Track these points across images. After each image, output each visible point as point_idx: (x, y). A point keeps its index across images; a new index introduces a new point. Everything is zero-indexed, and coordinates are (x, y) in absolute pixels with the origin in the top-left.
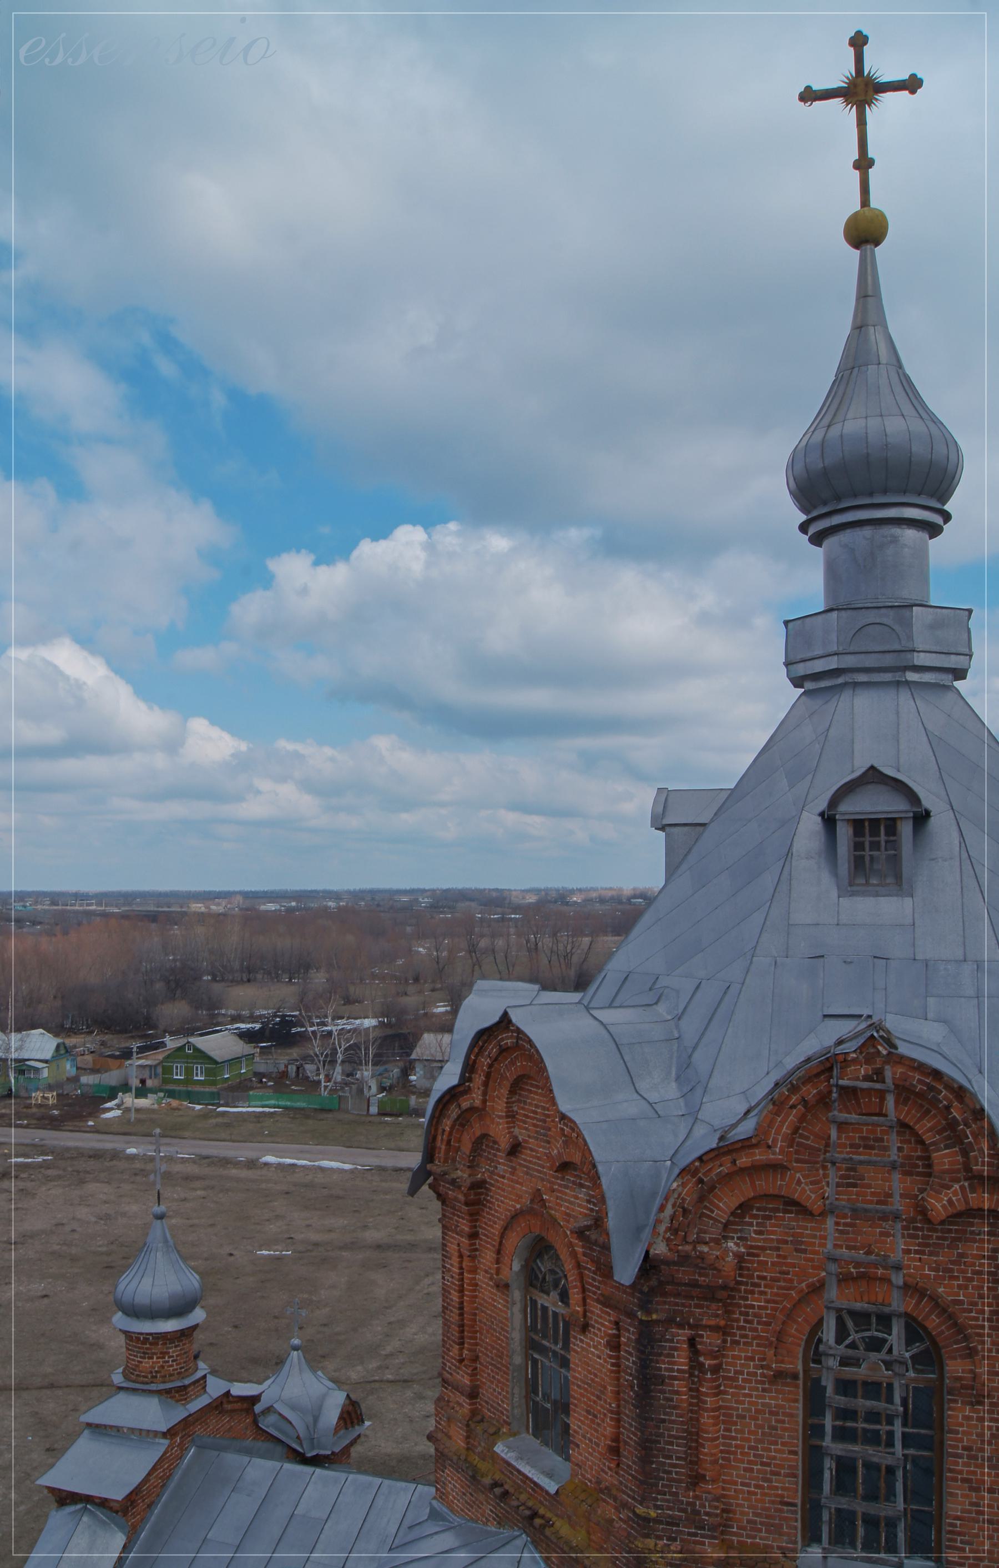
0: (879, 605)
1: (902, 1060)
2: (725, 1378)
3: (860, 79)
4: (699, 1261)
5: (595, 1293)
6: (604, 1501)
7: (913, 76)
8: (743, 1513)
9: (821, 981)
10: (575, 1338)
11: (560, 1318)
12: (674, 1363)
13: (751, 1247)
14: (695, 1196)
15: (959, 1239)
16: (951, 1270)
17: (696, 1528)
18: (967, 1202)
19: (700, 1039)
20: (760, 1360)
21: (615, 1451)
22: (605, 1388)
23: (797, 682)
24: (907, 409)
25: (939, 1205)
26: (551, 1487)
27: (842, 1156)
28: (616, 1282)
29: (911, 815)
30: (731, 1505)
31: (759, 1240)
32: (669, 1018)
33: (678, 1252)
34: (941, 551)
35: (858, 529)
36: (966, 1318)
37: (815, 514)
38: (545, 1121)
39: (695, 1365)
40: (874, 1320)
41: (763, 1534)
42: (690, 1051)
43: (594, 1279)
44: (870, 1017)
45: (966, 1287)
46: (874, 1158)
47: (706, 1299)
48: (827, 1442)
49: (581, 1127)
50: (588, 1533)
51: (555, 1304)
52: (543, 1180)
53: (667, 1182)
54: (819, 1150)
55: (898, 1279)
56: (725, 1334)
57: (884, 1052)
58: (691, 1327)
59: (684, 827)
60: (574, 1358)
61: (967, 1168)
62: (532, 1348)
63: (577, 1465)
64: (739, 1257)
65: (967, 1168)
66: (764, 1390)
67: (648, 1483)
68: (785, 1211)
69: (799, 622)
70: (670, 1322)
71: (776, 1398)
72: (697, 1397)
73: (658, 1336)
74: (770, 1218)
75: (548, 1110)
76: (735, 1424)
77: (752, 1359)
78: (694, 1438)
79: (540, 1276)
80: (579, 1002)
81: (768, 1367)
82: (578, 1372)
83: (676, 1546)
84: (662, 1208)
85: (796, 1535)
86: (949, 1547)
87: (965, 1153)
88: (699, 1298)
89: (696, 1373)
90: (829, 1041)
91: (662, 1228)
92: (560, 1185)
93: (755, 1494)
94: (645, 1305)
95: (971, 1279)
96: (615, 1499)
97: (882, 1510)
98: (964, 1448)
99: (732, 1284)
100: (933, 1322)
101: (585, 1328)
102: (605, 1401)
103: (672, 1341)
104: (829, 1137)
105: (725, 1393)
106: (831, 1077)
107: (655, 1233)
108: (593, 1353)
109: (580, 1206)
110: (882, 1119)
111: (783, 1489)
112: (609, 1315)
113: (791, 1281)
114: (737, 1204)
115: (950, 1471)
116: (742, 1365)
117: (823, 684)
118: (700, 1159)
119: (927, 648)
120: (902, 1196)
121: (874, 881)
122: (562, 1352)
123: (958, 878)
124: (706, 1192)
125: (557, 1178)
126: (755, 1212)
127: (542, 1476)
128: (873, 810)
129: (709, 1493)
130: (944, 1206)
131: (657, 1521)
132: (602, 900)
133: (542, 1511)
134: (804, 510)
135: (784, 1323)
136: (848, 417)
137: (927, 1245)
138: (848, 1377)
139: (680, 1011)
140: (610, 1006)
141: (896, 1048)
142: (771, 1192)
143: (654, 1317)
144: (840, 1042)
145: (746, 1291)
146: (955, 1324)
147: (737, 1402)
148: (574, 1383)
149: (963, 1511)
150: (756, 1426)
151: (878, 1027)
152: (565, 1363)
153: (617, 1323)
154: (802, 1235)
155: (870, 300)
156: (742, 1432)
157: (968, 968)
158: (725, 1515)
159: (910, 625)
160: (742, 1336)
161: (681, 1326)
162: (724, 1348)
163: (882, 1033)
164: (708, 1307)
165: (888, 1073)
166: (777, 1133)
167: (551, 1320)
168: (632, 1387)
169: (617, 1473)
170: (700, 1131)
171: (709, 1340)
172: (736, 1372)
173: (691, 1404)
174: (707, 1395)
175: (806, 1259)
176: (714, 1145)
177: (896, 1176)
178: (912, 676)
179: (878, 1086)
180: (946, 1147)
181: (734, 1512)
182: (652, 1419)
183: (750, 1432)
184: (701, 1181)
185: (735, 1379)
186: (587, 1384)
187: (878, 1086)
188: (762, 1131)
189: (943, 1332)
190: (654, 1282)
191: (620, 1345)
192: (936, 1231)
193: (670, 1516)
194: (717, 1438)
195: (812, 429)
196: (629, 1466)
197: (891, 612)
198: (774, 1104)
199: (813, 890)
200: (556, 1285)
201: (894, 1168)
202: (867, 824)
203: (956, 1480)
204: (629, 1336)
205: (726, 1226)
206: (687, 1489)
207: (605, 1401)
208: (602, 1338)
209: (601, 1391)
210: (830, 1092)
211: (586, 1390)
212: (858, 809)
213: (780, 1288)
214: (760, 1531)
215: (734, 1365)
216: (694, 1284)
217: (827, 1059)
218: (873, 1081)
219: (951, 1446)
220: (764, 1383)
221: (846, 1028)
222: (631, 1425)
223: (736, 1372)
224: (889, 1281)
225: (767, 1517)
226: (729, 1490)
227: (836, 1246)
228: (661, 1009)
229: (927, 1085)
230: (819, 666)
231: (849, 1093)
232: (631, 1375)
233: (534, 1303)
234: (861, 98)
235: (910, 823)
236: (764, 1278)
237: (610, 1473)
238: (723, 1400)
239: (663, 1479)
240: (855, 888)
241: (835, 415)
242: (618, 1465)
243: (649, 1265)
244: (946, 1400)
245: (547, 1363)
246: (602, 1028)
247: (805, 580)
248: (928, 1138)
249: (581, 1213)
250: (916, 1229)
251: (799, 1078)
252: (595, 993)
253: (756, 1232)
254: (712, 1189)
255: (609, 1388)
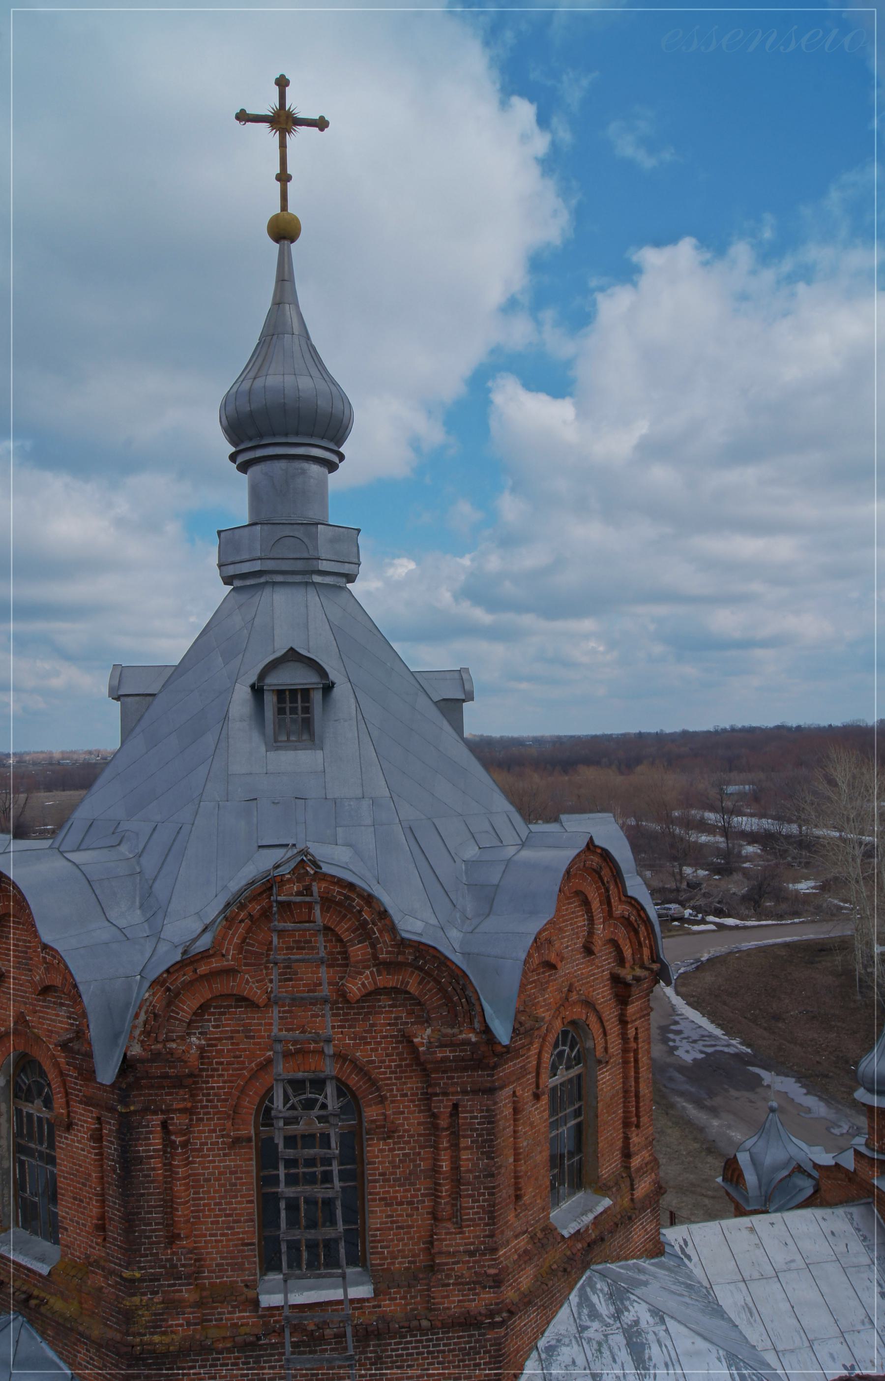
0: (292, 522)
1: (325, 877)
2: (193, 1150)
3: (282, 112)
4: (169, 1056)
5: (77, 1096)
6: (93, 1272)
7: (322, 118)
8: (212, 1259)
9: (255, 819)
10: (61, 1137)
11: (45, 1122)
12: (151, 1145)
13: (210, 1039)
14: (164, 1003)
15: (369, 1013)
16: (366, 1038)
17: (175, 1279)
18: (375, 983)
19: (159, 872)
20: (221, 1131)
21: (101, 1228)
22: (90, 1175)
23: (227, 580)
24: (314, 372)
25: (355, 988)
26: (44, 1269)
27: (283, 957)
28: (100, 1083)
29: (321, 686)
30: (202, 1254)
31: (216, 1033)
32: (131, 856)
33: (151, 1050)
34: (335, 481)
35: (276, 461)
36: (378, 1073)
37: (242, 447)
38: (26, 953)
39: (168, 1144)
40: (308, 1085)
41: (229, 1273)
42: (150, 882)
43: (76, 1084)
44: (294, 845)
45: (377, 1050)
46: (307, 957)
47: (174, 1087)
48: (282, 1188)
49: (62, 954)
50: (80, 1303)
51: (39, 1111)
52: (25, 1003)
53: (138, 994)
54: (262, 954)
55: (329, 1050)
56: (191, 1114)
57: (312, 872)
58: (163, 1112)
59: (137, 696)
60: (59, 1154)
61: (375, 957)
62: (19, 1152)
63: (67, 1246)
64: (201, 1048)
65: (375, 957)
66: (225, 1155)
67: (131, 1250)
68: (237, 1007)
69: (230, 532)
70: (146, 1110)
71: (235, 1160)
72: (170, 1170)
73: (135, 1124)
74: (224, 1013)
75: (30, 942)
76: (203, 1187)
77: (214, 1131)
78: (169, 1205)
79: (24, 1088)
80: (50, 847)
81: (228, 1136)
82: (64, 1165)
83: (158, 1298)
84: (137, 1016)
85: (255, 1270)
86: (372, 1253)
87: (373, 946)
88: (169, 1088)
89: (169, 1150)
90: (269, 865)
91: (137, 1032)
92: (42, 1007)
93: (221, 1241)
94: (124, 1100)
95: (380, 1043)
96: (103, 1269)
97: (329, 1233)
98: (380, 1175)
99: (196, 1072)
100: (354, 1080)
101: (69, 1127)
102: (90, 1187)
103: (147, 1126)
104: (271, 942)
105: (193, 1162)
106: (272, 895)
107: (131, 1038)
108: (77, 1147)
109: (60, 1022)
110: (312, 924)
111: (243, 1233)
112: (92, 1112)
113: (243, 1062)
114: (198, 1005)
115: (371, 1194)
116: (206, 1137)
117: (248, 582)
118: (168, 971)
119: (328, 557)
120: (330, 984)
121: (293, 738)
122: (48, 1151)
123: (356, 735)
124: (173, 998)
125: (39, 1000)
126: (212, 1010)
127: (34, 1262)
128: (293, 682)
129: (184, 1248)
130: (359, 989)
131: (141, 1280)
133: (36, 1293)
134: (233, 443)
135: (239, 1098)
136: (269, 372)
137: (347, 1020)
138: (290, 1133)
139: (140, 850)
140: (78, 849)
141: (321, 868)
142: (226, 992)
143: (132, 1108)
144: (276, 867)
145: (207, 1076)
146: (370, 1079)
147: (203, 1168)
148: (60, 1176)
149: (381, 1223)
150: (220, 1185)
151: (305, 852)
152: (52, 1160)
153: (99, 1119)
154: (250, 1024)
155: (287, 284)
156: (209, 1192)
157: (366, 803)
158: (197, 1264)
159: (316, 538)
160: (205, 1114)
161: (155, 1113)
162: (191, 1126)
163: (309, 857)
164: (177, 1094)
165: (315, 889)
166: (230, 943)
167: (36, 1125)
168: (114, 1171)
169: (103, 1247)
170: (163, 948)
171: (178, 1121)
172: (202, 1144)
173: (165, 1177)
174: (178, 1166)
175: (254, 1044)
176: (178, 958)
177: (323, 969)
178: (317, 579)
179: (308, 899)
180: (359, 942)
181: (204, 1260)
182: (133, 1195)
183: (215, 1191)
184: (168, 989)
185: (201, 1150)
186: (73, 1174)
187: (308, 899)
188: (217, 943)
189: (361, 1087)
190: (131, 1079)
191: (102, 1137)
192: (353, 1008)
193: (152, 1274)
194: (187, 1202)
195: (241, 379)
196: (115, 1239)
197: (302, 528)
198: (226, 920)
199: (246, 749)
200: (40, 1094)
201: (322, 963)
202: (287, 693)
203: (374, 1200)
204: (110, 1127)
205: (189, 1024)
206: (166, 1248)
207: (90, 1187)
208: (85, 1133)
209: (86, 1179)
210: (271, 907)
211: (72, 1180)
212: (280, 682)
213: (234, 1069)
214: (227, 1270)
215: (200, 1138)
216: (165, 1076)
217: (268, 881)
218: (304, 895)
219: (371, 1175)
220: (224, 1149)
221: (279, 855)
222: (115, 1203)
223: (202, 1144)
224: (323, 1052)
225: (232, 1258)
226: (200, 1242)
227: (280, 1030)
228: (124, 848)
229: (344, 895)
230: (246, 568)
231: (285, 906)
232: (113, 1160)
233: (19, 1112)
234: (284, 126)
235: (320, 692)
236: (222, 1063)
237: (97, 1247)
238: (192, 1169)
239: (145, 1244)
240: (279, 744)
241: (259, 370)
242: (104, 1240)
243: (127, 1065)
244: (364, 1140)
245: (34, 1162)
246: (75, 867)
247: (233, 498)
248: (346, 937)
249: (62, 1028)
250: (338, 1008)
251: (246, 898)
252: (63, 839)
253: (214, 1026)
254: (178, 994)
255: (94, 1175)
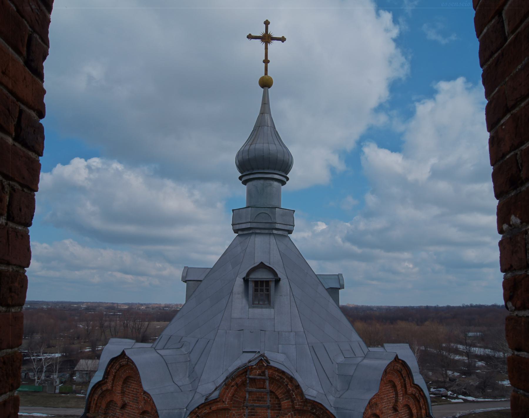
1: (272, 368)
7: (283, 37)
23: (236, 231)
24: (277, 142)
44: (259, 352)
57: (266, 365)
61: (293, 407)
65: (293, 407)
87: (292, 401)
104: (245, 397)
118: (198, 407)
119: (280, 222)
132: (153, 309)
140: (163, 349)
144: (250, 362)
165: (267, 373)
170: (197, 396)
176: (203, 402)
178: (275, 232)
179: (263, 377)
187: (263, 377)
188: (221, 395)
197: (269, 209)
210: (246, 380)
212: (256, 277)
228: (183, 349)
229: (280, 377)
230: (244, 226)
231: (253, 380)
235: (274, 282)
